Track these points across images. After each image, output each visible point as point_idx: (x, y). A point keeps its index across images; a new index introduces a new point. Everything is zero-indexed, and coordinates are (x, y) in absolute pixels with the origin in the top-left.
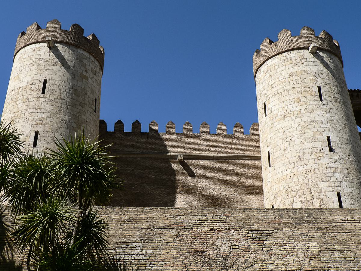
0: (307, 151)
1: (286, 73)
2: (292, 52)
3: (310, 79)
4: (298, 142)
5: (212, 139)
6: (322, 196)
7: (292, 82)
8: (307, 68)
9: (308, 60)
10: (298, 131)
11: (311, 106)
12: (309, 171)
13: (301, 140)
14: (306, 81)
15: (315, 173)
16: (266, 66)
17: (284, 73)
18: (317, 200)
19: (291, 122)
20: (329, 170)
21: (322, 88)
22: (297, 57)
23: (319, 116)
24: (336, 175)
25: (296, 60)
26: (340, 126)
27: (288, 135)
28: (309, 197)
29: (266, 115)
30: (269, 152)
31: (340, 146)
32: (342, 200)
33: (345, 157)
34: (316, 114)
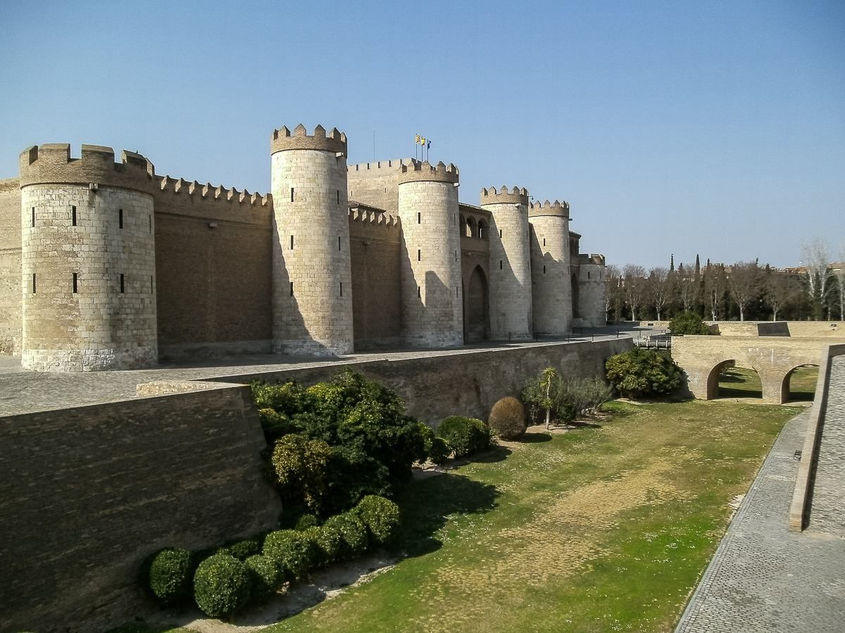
29: (419, 223)
30: (419, 251)
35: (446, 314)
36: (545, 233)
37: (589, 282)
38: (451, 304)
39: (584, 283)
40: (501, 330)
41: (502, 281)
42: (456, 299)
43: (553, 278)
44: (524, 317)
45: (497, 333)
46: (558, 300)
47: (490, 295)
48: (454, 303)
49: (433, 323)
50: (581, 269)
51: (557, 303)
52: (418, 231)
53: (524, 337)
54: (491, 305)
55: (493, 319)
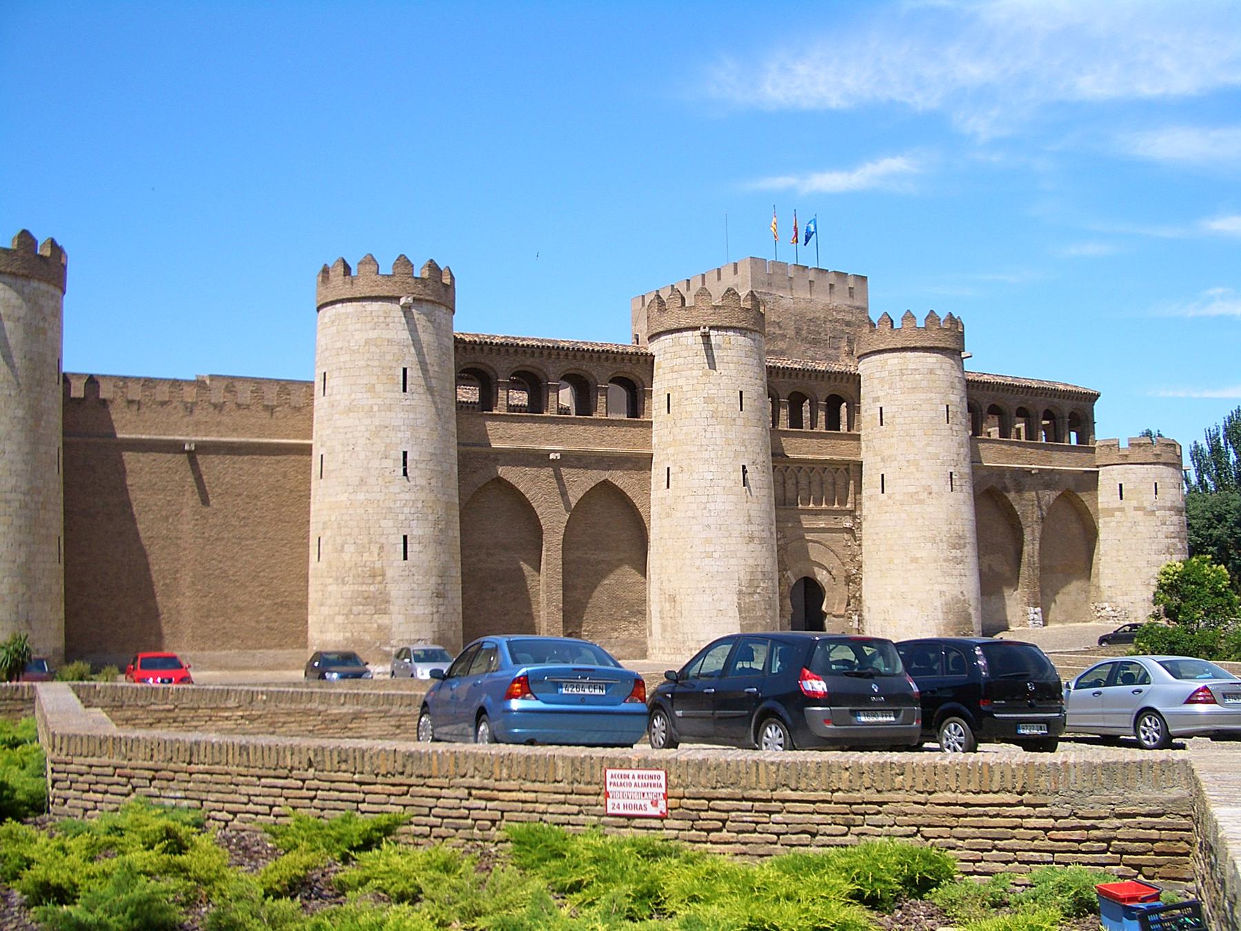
0: (372, 471)
1: (360, 337)
4: (362, 456)
5: (241, 412)
6: (383, 540)
7: (367, 356)
8: (390, 334)
11: (387, 402)
14: (388, 357)
20: (398, 504)
22: (381, 313)
23: (398, 418)
24: (406, 510)
25: (378, 317)
26: (423, 434)
27: (352, 441)
28: (366, 541)
33: (424, 482)
34: (393, 414)
35: (368, 600)
36: (880, 394)
37: (1122, 510)
38: (383, 575)
39: (1110, 512)
41: (668, 515)
44: (723, 606)
45: (662, 644)
46: (914, 560)
48: (390, 573)
49: (340, 619)
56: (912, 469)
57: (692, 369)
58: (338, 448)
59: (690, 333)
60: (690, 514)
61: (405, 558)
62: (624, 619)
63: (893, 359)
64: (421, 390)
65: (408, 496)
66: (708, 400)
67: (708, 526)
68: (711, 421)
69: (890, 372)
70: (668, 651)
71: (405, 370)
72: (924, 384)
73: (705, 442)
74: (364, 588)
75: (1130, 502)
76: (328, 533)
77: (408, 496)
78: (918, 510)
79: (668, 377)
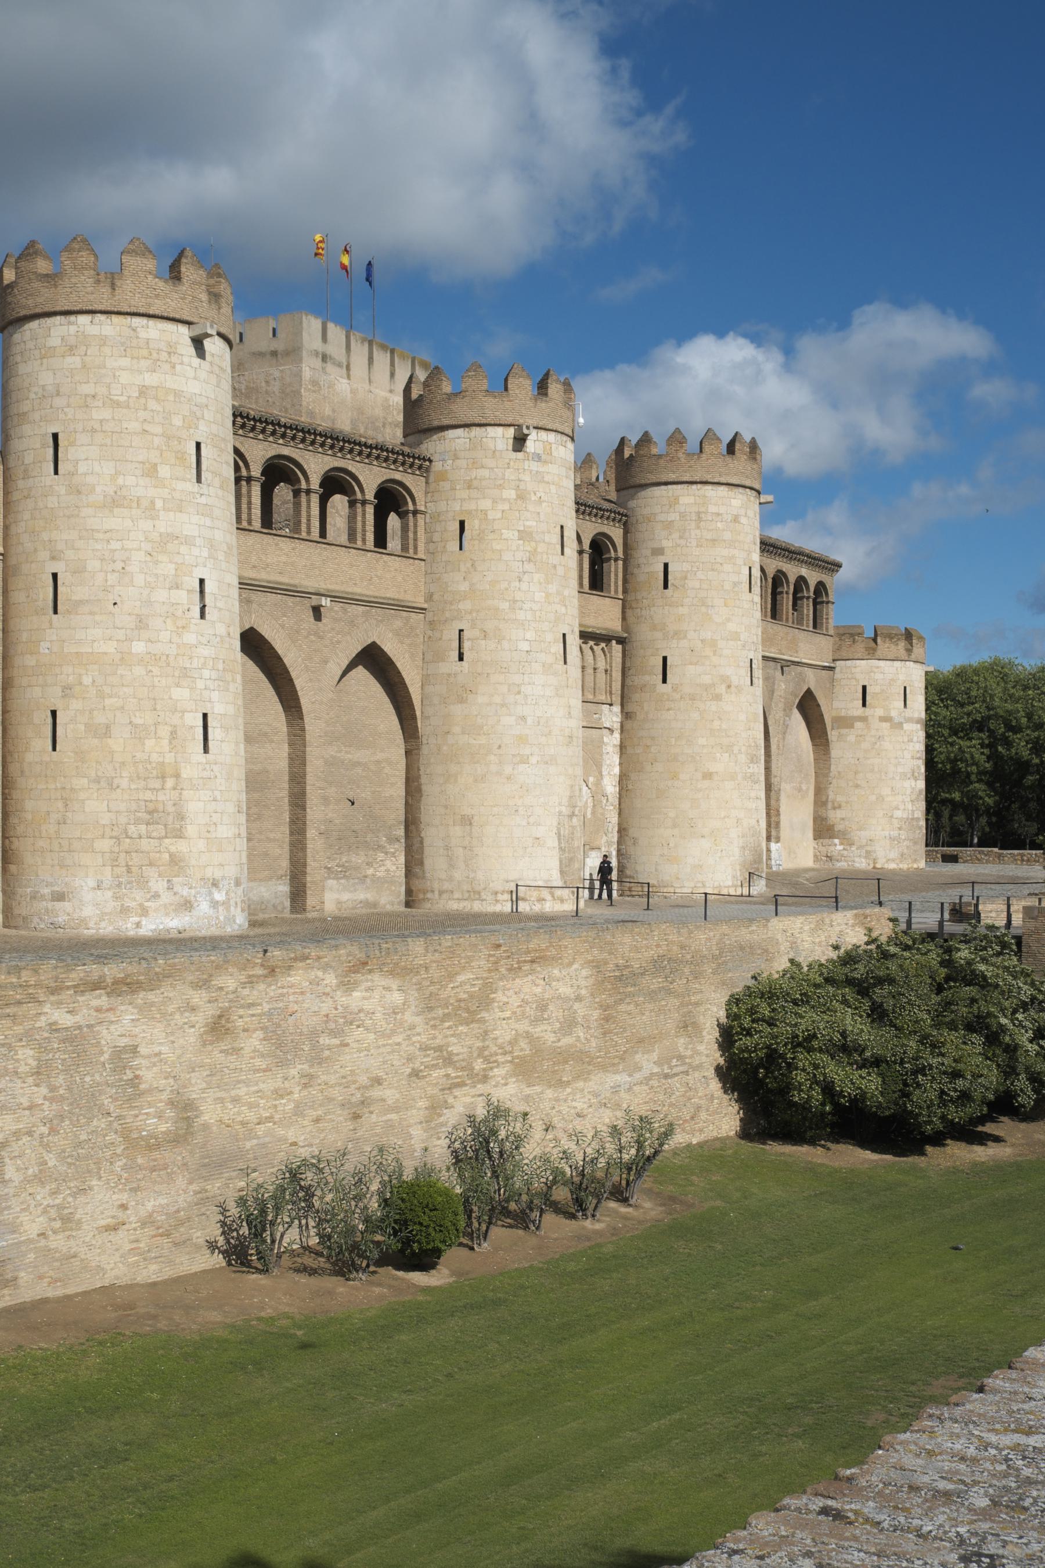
2: (152, 322)
3: (184, 417)
9: (186, 360)
10: (143, 553)
12: (158, 657)
13: (149, 579)
15: (168, 665)
16: (73, 329)
17: (125, 378)
18: (166, 727)
19: (128, 523)
20: (195, 663)
21: (203, 446)
30: (55, 576)
31: (218, 605)
32: (210, 730)
35: (152, 814)
36: (665, 543)
37: (864, 719)
38: (177, 776)
40: (458, 875)
41: (462, 700)
42: (202, 757)
43: (693, 698)
45: (447, 886)
46: (708, 776)
47: (425, 750)
50: (838, 675)
51: (706, 783)
52: (52, 502)
53: (541, 900)
54: (424, 788)
55: (432, 835)
56: (708, 652)
57: (501, 487)
58: (93, 565)
59: (500, 430)
60: (497, 699)
61: (206, 750)
62: (380, 848)
63: (687, 497)
64: (217, 482)
65: (206, 651)
66: (525, 535)
67: (523, 718)
68: (528, 567)
69: (683, 515)
70: (457, 895)
71: (198, 445)
72: (727, 535)
73: (519, 596)
74: (149, 796)
75: (875, 711)
76: (75, 705)
77: (206, 651)
78: (714, 708)
79: (464, 494)
